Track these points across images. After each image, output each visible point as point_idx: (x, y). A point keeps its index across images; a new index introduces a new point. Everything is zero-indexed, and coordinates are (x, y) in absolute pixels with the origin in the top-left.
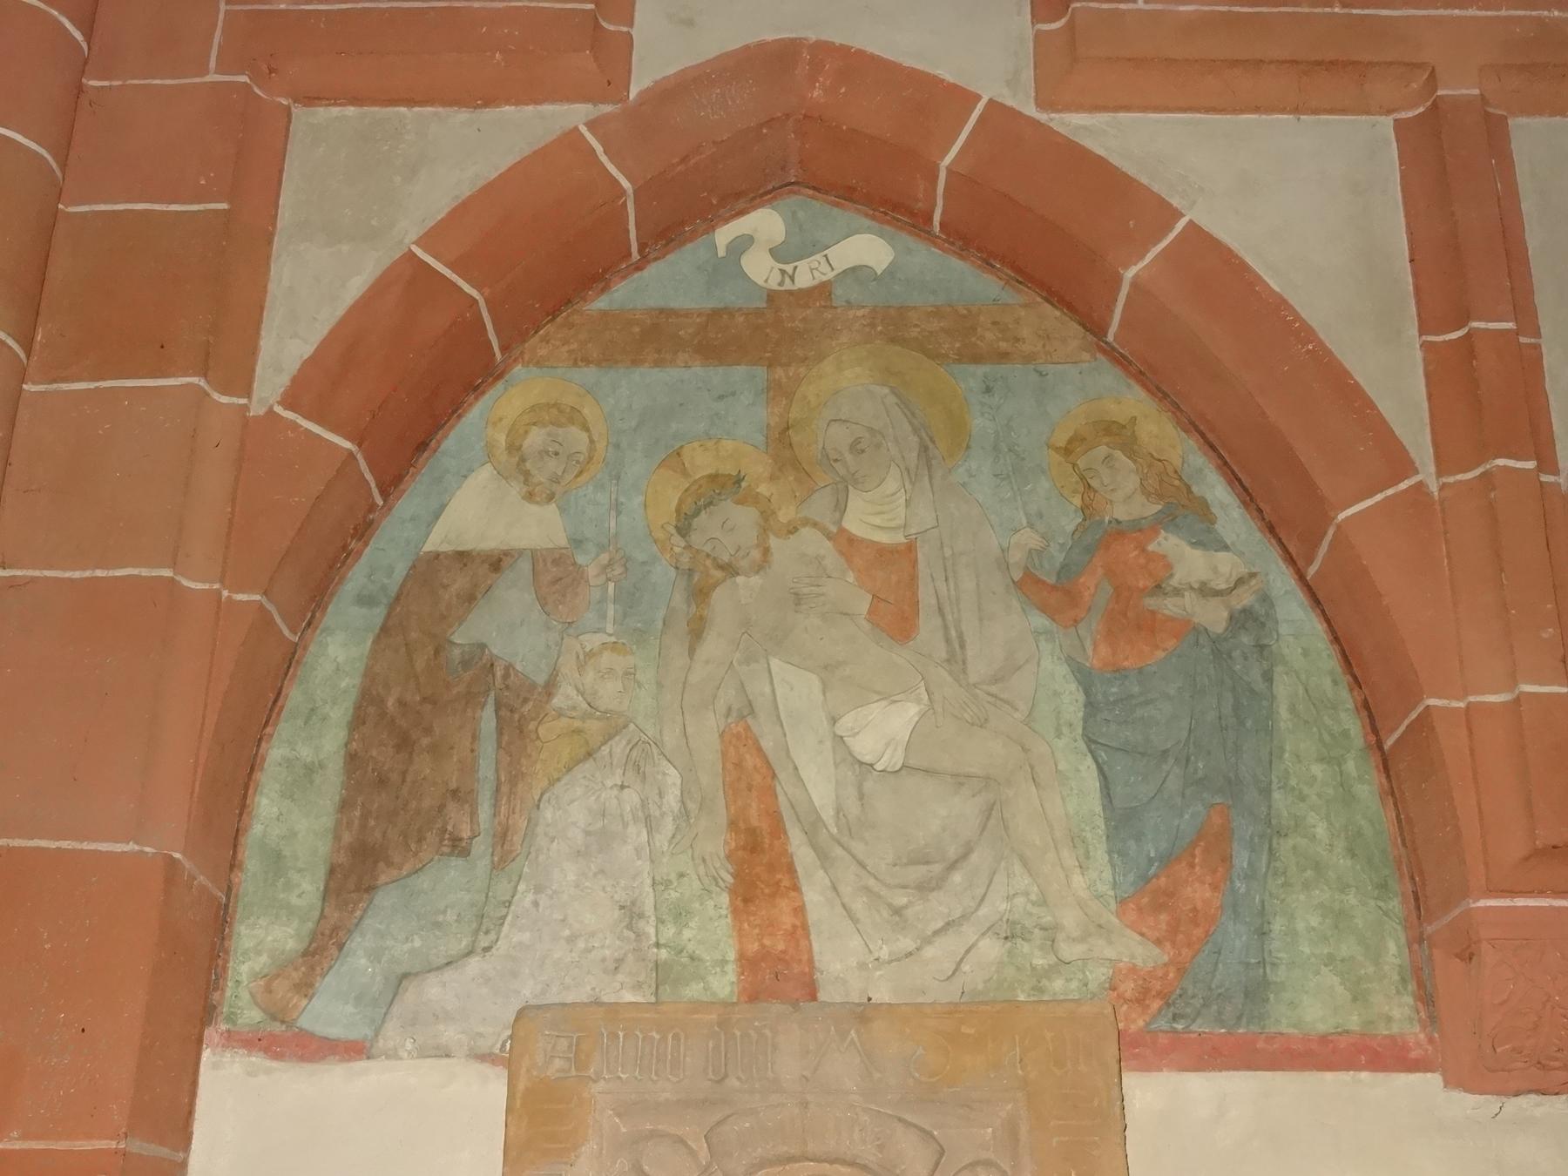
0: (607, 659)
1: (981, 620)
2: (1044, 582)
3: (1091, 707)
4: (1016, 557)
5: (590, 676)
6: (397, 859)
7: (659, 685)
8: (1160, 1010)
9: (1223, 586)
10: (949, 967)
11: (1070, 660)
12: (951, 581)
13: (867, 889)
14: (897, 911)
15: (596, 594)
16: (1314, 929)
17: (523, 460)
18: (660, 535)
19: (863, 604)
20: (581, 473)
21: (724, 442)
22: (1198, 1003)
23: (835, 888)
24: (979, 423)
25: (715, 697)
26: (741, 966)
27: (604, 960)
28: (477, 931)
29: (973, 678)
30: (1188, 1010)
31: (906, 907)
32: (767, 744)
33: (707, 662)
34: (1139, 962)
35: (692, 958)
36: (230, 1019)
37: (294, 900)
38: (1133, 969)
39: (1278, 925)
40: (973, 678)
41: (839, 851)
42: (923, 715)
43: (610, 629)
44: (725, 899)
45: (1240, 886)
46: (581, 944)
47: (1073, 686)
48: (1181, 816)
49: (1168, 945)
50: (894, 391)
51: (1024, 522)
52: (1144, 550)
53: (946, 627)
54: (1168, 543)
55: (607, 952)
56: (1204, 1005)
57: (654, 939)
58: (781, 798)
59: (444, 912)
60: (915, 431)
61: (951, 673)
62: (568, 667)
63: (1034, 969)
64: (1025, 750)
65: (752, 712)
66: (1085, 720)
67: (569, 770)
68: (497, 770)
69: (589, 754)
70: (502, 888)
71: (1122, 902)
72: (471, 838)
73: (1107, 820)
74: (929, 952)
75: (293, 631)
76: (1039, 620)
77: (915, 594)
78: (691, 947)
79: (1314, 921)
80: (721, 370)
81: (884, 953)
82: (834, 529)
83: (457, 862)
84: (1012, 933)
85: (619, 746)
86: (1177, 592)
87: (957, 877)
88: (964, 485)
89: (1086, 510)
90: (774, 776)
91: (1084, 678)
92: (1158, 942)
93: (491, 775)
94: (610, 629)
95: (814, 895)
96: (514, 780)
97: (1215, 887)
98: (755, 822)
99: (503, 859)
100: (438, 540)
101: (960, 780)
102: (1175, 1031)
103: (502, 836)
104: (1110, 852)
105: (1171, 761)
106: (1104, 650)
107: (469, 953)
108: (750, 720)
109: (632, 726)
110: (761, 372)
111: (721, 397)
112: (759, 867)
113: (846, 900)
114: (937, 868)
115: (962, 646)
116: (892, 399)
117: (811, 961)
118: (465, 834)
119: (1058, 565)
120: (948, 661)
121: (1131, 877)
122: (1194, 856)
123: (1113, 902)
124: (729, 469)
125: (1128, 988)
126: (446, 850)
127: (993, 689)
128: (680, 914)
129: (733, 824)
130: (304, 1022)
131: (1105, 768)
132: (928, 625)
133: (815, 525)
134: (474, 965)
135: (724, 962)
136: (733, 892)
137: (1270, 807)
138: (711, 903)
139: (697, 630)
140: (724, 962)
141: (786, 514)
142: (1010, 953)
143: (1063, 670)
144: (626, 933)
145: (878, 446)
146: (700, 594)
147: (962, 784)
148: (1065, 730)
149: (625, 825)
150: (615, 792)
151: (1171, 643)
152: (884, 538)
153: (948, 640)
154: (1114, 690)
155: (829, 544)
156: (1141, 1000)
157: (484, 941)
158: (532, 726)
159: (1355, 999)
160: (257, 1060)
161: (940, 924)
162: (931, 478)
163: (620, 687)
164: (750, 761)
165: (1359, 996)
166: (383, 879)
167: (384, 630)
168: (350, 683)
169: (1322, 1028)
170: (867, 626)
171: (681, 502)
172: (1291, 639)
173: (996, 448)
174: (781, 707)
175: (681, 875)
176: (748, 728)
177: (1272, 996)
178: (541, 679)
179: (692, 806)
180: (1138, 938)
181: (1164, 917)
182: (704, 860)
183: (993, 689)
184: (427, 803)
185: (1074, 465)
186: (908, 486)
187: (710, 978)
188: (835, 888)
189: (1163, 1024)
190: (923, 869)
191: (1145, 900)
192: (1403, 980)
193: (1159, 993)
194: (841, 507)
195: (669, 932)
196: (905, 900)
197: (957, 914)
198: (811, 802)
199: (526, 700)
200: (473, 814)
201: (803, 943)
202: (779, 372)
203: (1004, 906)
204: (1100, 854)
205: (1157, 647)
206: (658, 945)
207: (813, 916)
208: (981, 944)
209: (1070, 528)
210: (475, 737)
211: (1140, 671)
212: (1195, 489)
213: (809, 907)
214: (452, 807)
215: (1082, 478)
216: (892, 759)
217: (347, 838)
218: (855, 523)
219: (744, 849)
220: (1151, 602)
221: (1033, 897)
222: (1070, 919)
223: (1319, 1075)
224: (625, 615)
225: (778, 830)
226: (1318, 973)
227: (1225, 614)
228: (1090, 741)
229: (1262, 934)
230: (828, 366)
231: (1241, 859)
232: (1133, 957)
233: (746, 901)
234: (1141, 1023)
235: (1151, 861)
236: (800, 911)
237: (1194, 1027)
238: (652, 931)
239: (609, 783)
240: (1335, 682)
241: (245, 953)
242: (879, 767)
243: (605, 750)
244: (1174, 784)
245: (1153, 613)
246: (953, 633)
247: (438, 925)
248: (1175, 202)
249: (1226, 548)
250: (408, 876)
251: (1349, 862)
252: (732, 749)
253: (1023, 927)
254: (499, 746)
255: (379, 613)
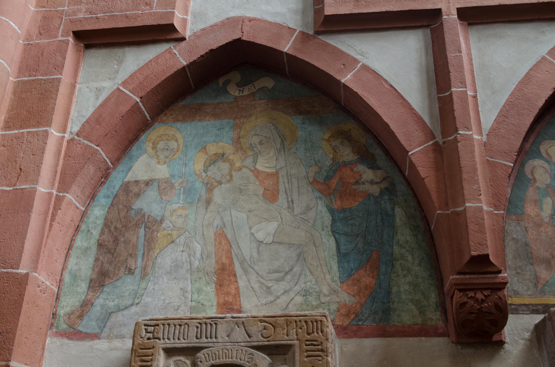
0: (180, 212)
1: (299, 195)
2: (319, 182)
3: (334, 221)
4: (311, 174)
5: (174, 218)
6: (111, 276)
7: (196, 219)
8: (354, 318)
9: (379, 181)
10: (284, 306)
11: (327, 206)
12: (290, 183)
13: (259, 281)
14: (268, 288)
15: (177, 192)
16: (406, 290)
17: (157, 152)
18: (198, 173)
19: (261, 191)
20: (174, 155)
21: (219, 143)
22: (366, 315)
23: (249, 281)
24: (300, 133)
25: (213, 222)
26: (218, 307)
27: (174, 306)
28: (134, 298)
29: (296, 213)
30: (363, 318)
31: (271, 287)
32: (229, 236)
33: (211, 212)
34: (347, 302)
35: (202, 305)
36: (57, 327)
37: (79, 290)
38: (345, 305)
39: (395, 289)
40: (296, 213)
41: (251, 270)
42: (279, 226)
43: (181, 202)
44: (214, 285)
45: (382, 277)
46: (167, 301)
47: (328, 214)
48: (363, 255)
49: (357, 297)
50: (273, 125)
51: (314, 163)
52: (352, 170)
53: (287, 198)
54: (361, 168)
55: (175, 304)
56: (368, 316)
57: (190, 299)
58: (233, 253)
59: (125, 292)
60: (280, 137)
61: (288, 212)
62: (167, 214)
63: (312, 305)
64: (312, 235)
65: (225, 226)
66: (332, 225)
67: (167, 246)
68: (144, 248)
69: (173, 242)
70: (143, 285)
71: (342, 283)
72: (135, 269)
73: (338, 257)
74: (278, 301)
75: (83, 206)
76: (317, 194)
77: (278, 187)
78: (202, 301)
79: (407, 287)
80: (219, 121)
81: (264, 302)
82: (253, 168)
83: (130, 276)
84: (306, 293)
85: (182, 239)
86: (363, 183)
87: (289, 277)
88: (295, 153)
89: (334, 159)
90: (231, 246)
91: (331, 211)
92: (354, 296)
93: (142, 249)
94: (181, 202)
95: (242, 283)
96: (150, 249)
97: (373, 277)
98: (224, 261)
99: (144, 275)
100: (130, 177)
101: (290, 245)
102: (359, 325)
103: (144, 268)
104: (339, 267)
105: (360, 237)
106: (339, 203)
107: (132, 305)
108: (224, 229)
109: (187, 232)
110: (231, 121)
111: (219, 129)
112: (224, 275)
113: (252, 285)
114: (282, 274)
115: (293, 203)
116: (272, 128)
117: (240, 305)
118: (133, 268)
119: (324, 177)
120: (288, 208)
121: (345, 275)
122: (366, 267)
123: (339, 283)
124: (220, 151)
125: (343, 311)
126: (127, 273)
127: (302, 216)
128: (199, 291)
129: (217, 262)
130: (80, 328)
131: (338, 240)
132: (282, 198)
133: (247, 167)
134: (134, 309)
135: (212, 306)
136: (216, 284)
137: (392, 251)
138: (209, 288)
139: (208, 202)
140: (212, 306)
141: (238, 164)
142: (305, 301)
143: (324, 209)
144: (182, 297)
145: (268, 142)
146: (210, 189)
147: (291, 247)
148: (325, 229)
149: (183, 264)
150: (180, 253)
151: (360, 200)
152: (269, 170)
153: (288, 202)
154: (341, 215)
155: (251, 173)
156: (347, 315)
157: (137, 301)
158: (155, 233)
159: (420, 313)
160: (65, 340)
161: (282, 292)
162: (284, 151)
163: (183, 220)
164: (223, 242)
165: (422, 313)
166: (107, 282)
167: (112, 205)
168: (100, 222)
169: (409, 323)
170: (262, 198)
171: (205, 162)
172: (401, 197)
173: (305, 141)
174: (234, 224)
175: (200, 278)
176: (223, 231)
177: (392, 313)
178: (159, 219)
179: (204, 256)
180: (347, 295)
181: (356, 288)
182: (207, 274)
183: (302, 216)
184: (122, 258)
185: (331, 145)
186: (277, 154)
187: (208, 311)
188: (249, 281)
189: (354, 322)
190: (277, 274)
191: (350, 282)
192: (437, 307)
193: (354, 313)
194: (255, 162)
195: (195, 296)
196: (271, 285)
197: (288, 288)
198: (242, 254)
199: (154, 225)
200: (136, 261)
201: (238, 299)
202: (238, 121)
203: (303, 286)
204: (335, 267)
205: (356, 201)
206: (192, 301)
207: (241, 290)
208: (295, 298)
209: (329, 164)
210: (138, 238)
211: (350, 209)
212: (370, 151)
213: (240, 287)
214: (129, 259)
215: (333, 149)
216: (269, 239)
217: (96, 270)
218: (259, 167)
219: (220, 269)
220: (354, 187)
221: (313, 282)
222: (325, 290)
223: (408, 338)
224: (186, 198)
225: (232, 264)
226: (407, 305)
227: (379, 190)
228: (333, 232)
229: (389, 293)
230: (253, 118)
231: (383, 269)
232: (345, 301)
233: (220, 286)
234: (348, 322)
235: (352, 270)
236: (237, 289)
237: (366, 323)
238: (190, 297)
239: (178, 250)
240: (415, 210)
241: (63, 307)
242: (264, 242)
243: (178, 240)
244: (360, 245)
245: (355, 190)
246: (290, 199)
247: (123, 296)
248: (358, 57)
249: (380, 169)
250: (115, 281)
251: (419, 268)
252: (218, 239)
253: (310, 292)
254: (145, 239)
255: (110, 201)
